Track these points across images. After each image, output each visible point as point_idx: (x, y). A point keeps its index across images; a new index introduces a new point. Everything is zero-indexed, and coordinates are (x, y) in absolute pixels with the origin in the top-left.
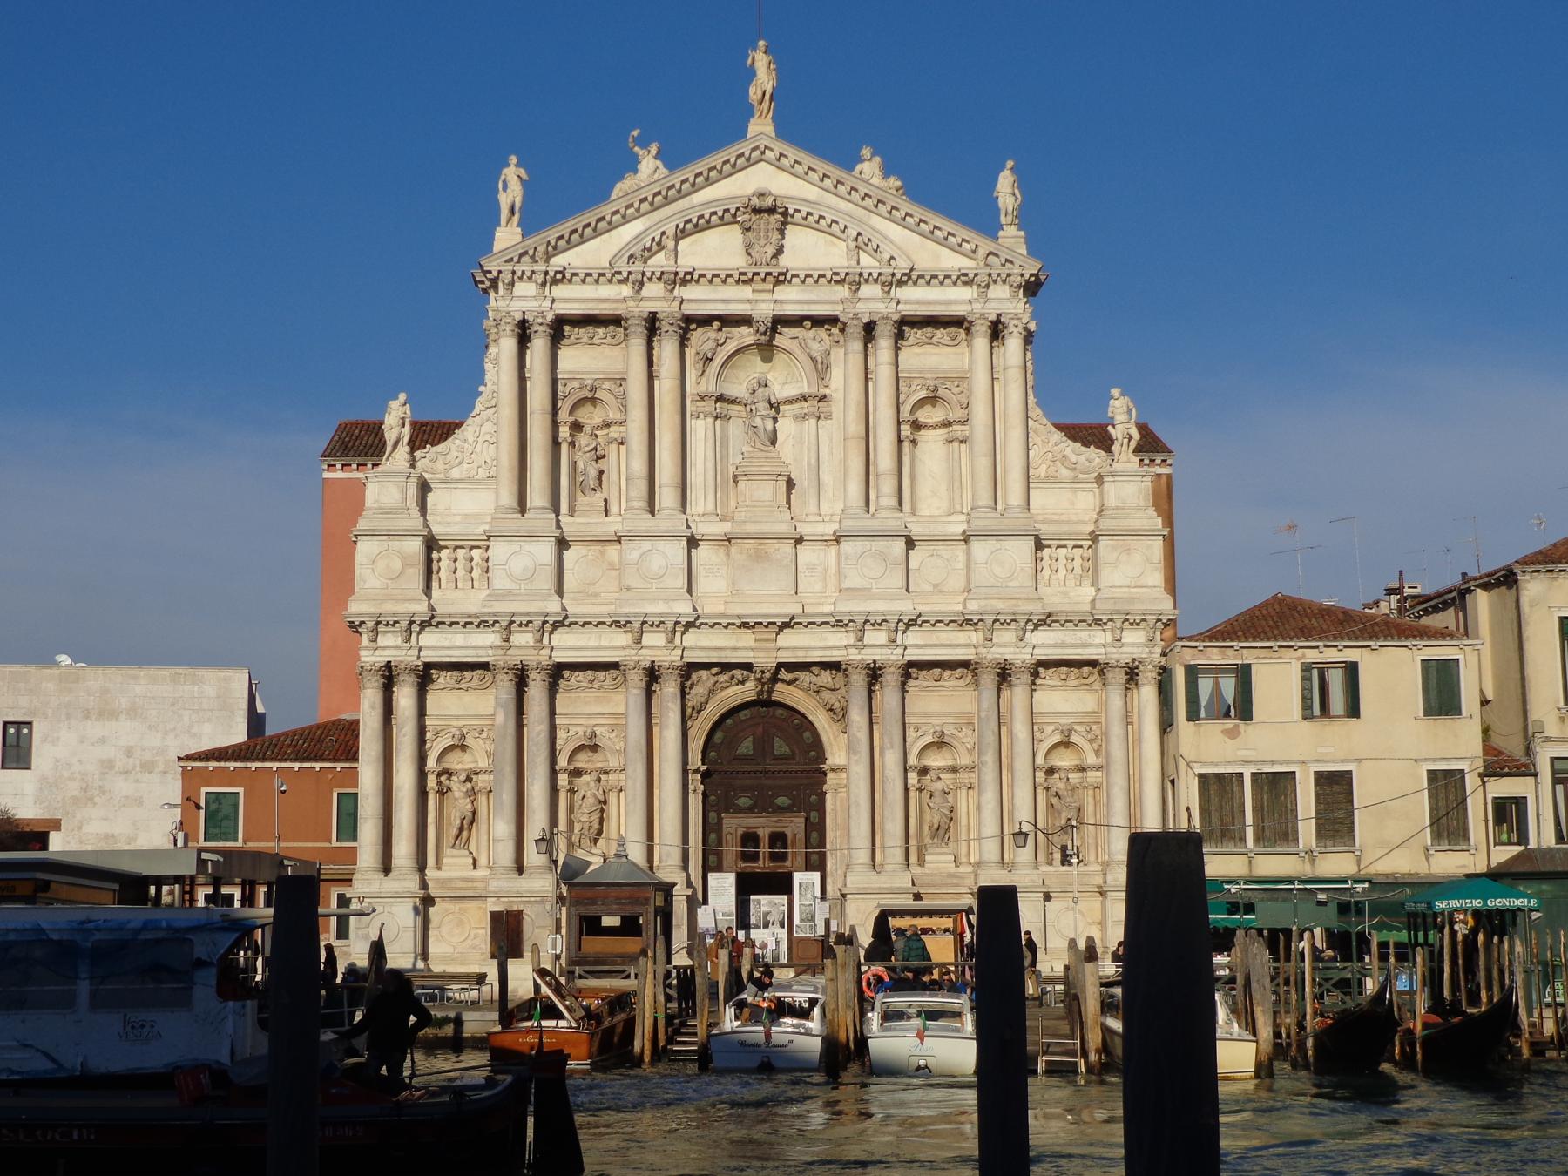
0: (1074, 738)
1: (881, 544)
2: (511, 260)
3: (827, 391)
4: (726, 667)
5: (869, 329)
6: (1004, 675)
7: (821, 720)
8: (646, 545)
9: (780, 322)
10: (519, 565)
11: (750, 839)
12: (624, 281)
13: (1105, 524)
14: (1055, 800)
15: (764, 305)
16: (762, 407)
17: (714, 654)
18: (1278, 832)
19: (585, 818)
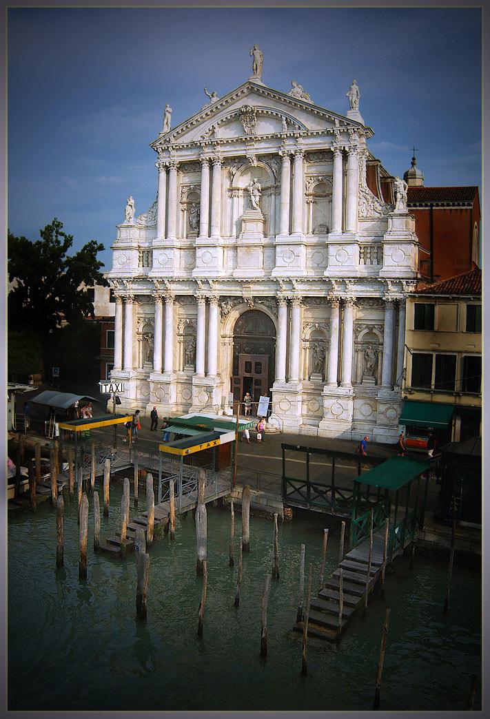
0: (374, 331)
1: (292, 248)
2: (161, 143)
3: (278, 184)
4: (236, 298)
5: (292, 157)
6: (342, 303)
7: (273, 318)
8: (204, 250)
9: (260, 157)
10: (161, 258)
11: (248, 364)
12: (200, 147)
13: (387, 237)
14: (366, 357)
15: (252, 151)
16: (256, 191)
17: (228, 292)
18: (446, 383)
19: (188, 353)
